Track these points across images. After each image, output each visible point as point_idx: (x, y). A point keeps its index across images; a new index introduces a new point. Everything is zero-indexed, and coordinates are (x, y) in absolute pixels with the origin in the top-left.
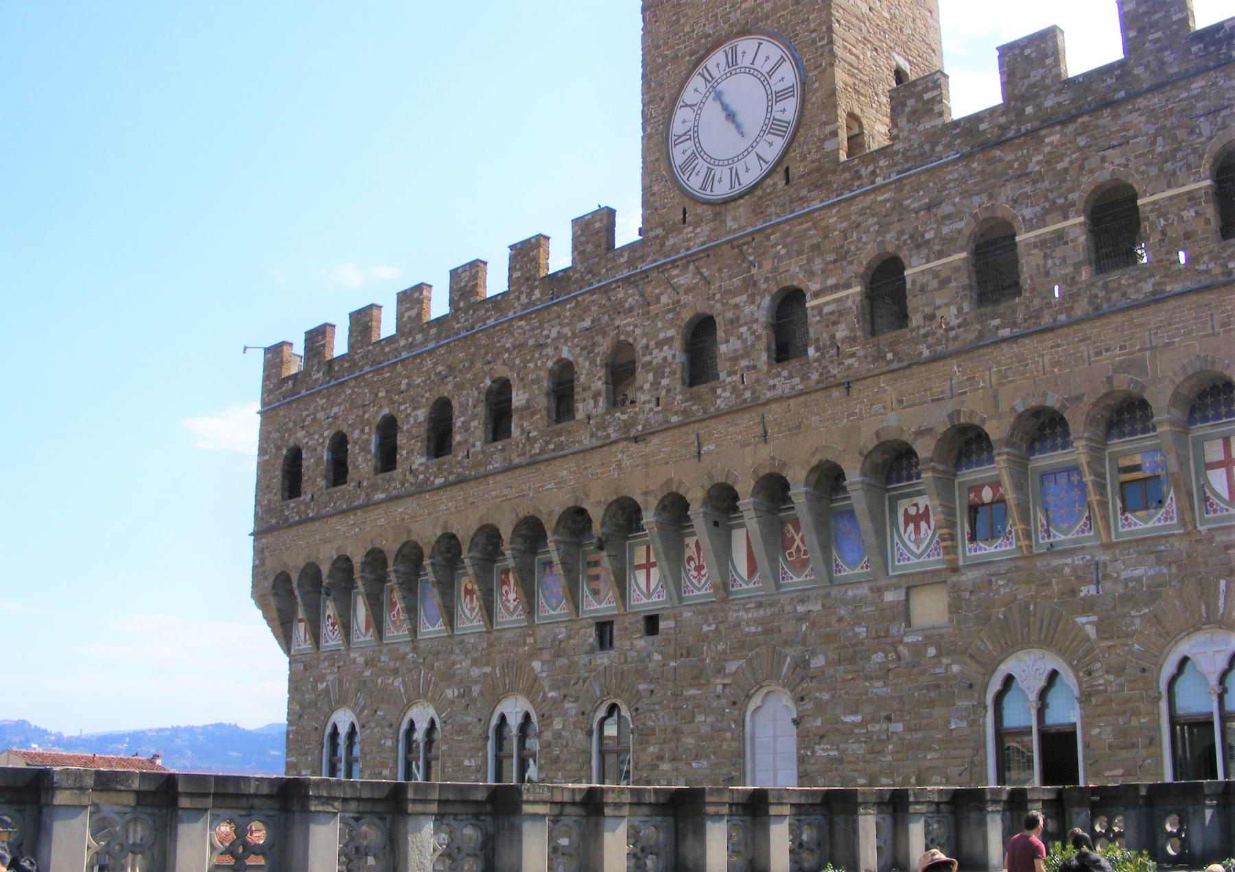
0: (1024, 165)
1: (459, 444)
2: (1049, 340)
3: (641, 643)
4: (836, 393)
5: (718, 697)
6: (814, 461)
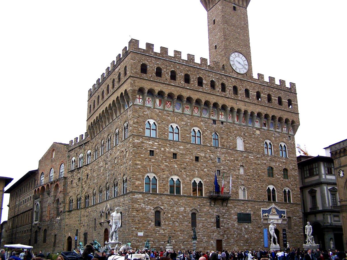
0: (272, 90)
1: (192, 83)
2: (275, 109)
3: (221, 125)
4: (254, 104)
5: (233, 135)
6: (251, 111)
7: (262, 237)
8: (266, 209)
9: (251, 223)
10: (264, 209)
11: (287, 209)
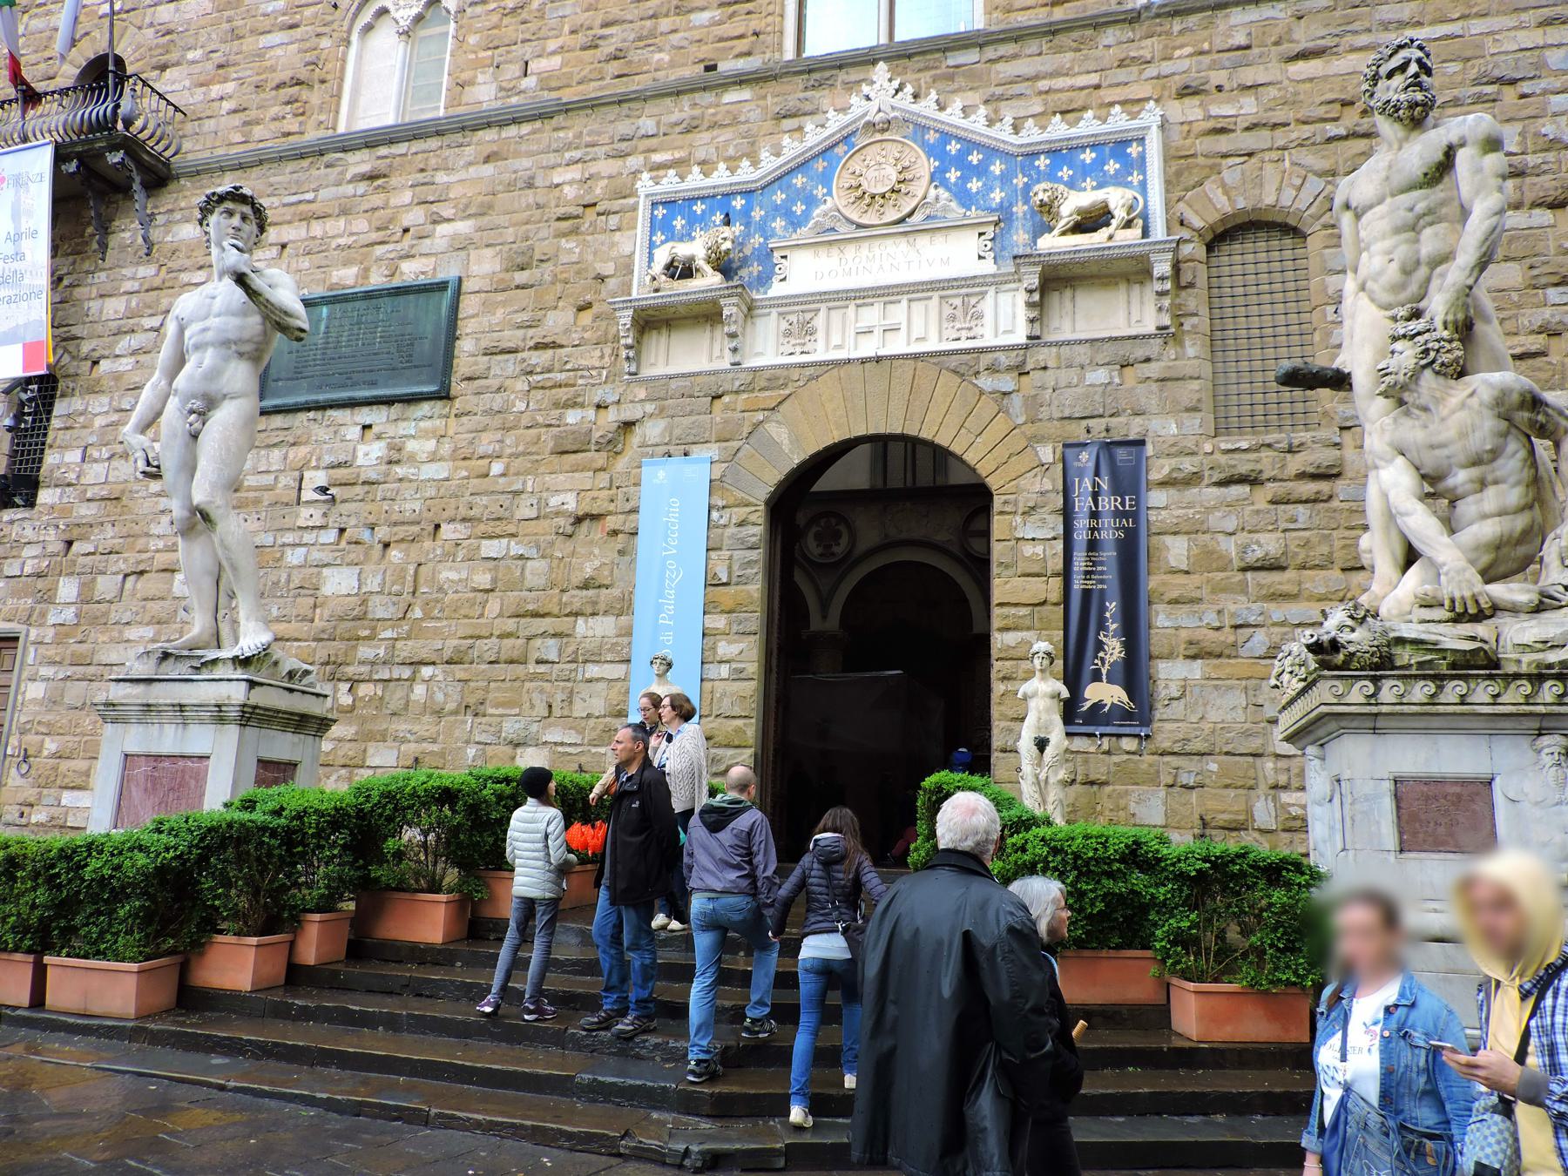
7: (586, 586)
8: (721, 177)
9: (444, 395)
10: (696, 180)
11: (1186, 92)
